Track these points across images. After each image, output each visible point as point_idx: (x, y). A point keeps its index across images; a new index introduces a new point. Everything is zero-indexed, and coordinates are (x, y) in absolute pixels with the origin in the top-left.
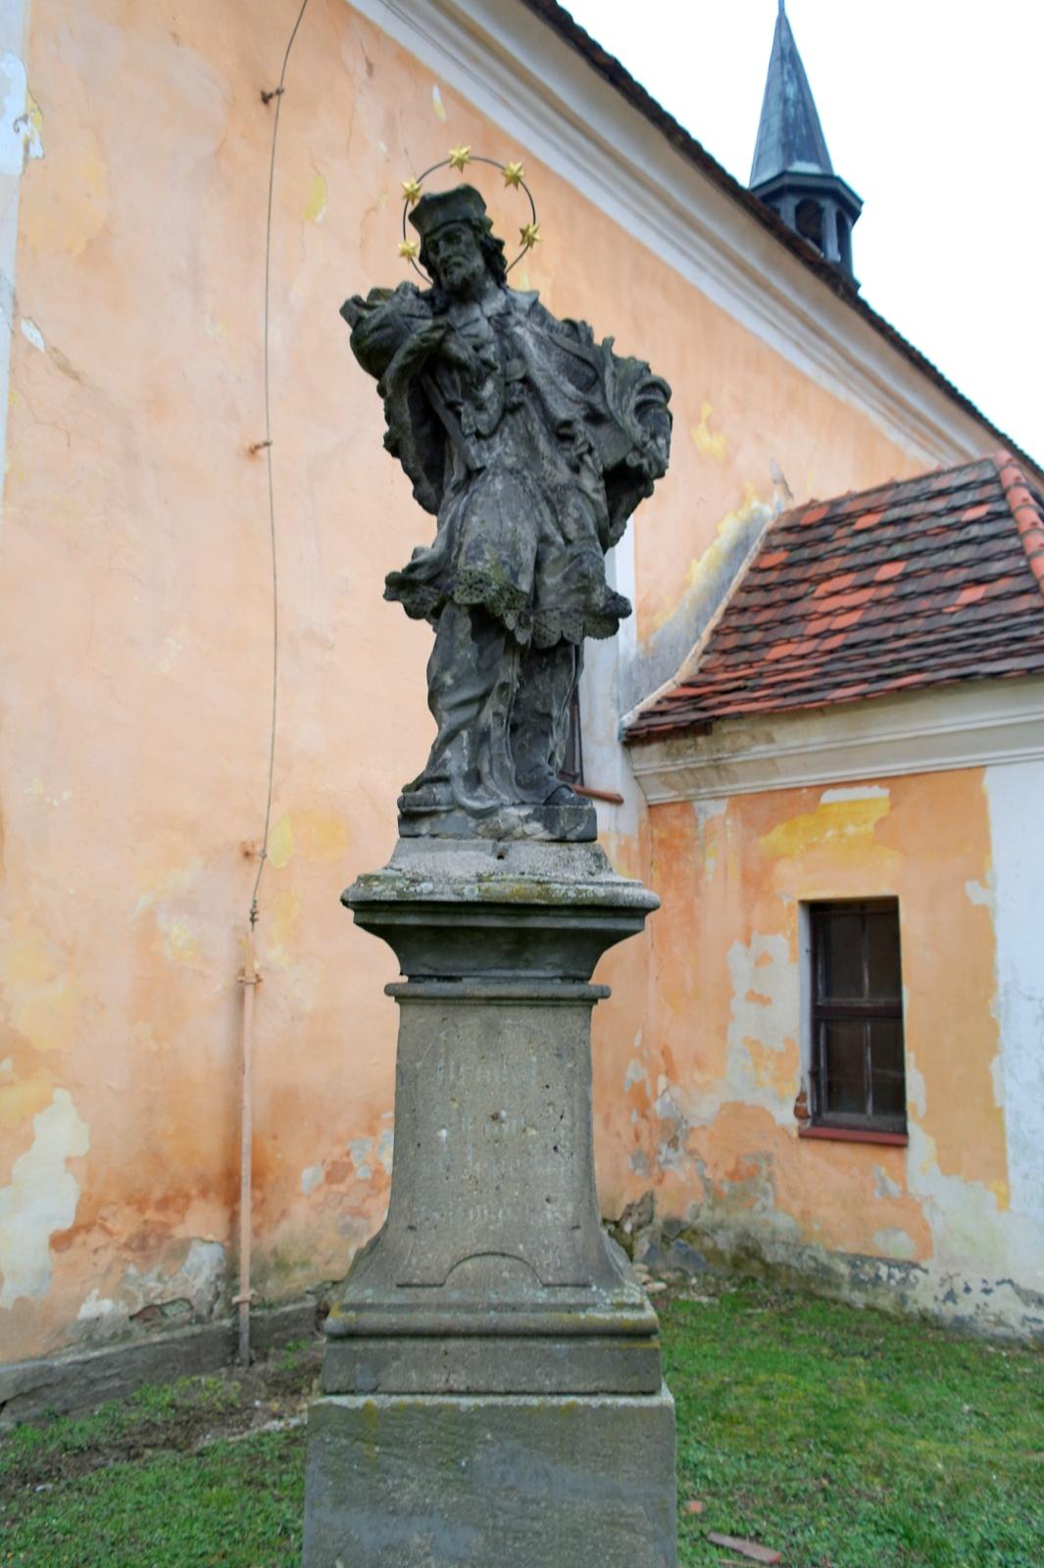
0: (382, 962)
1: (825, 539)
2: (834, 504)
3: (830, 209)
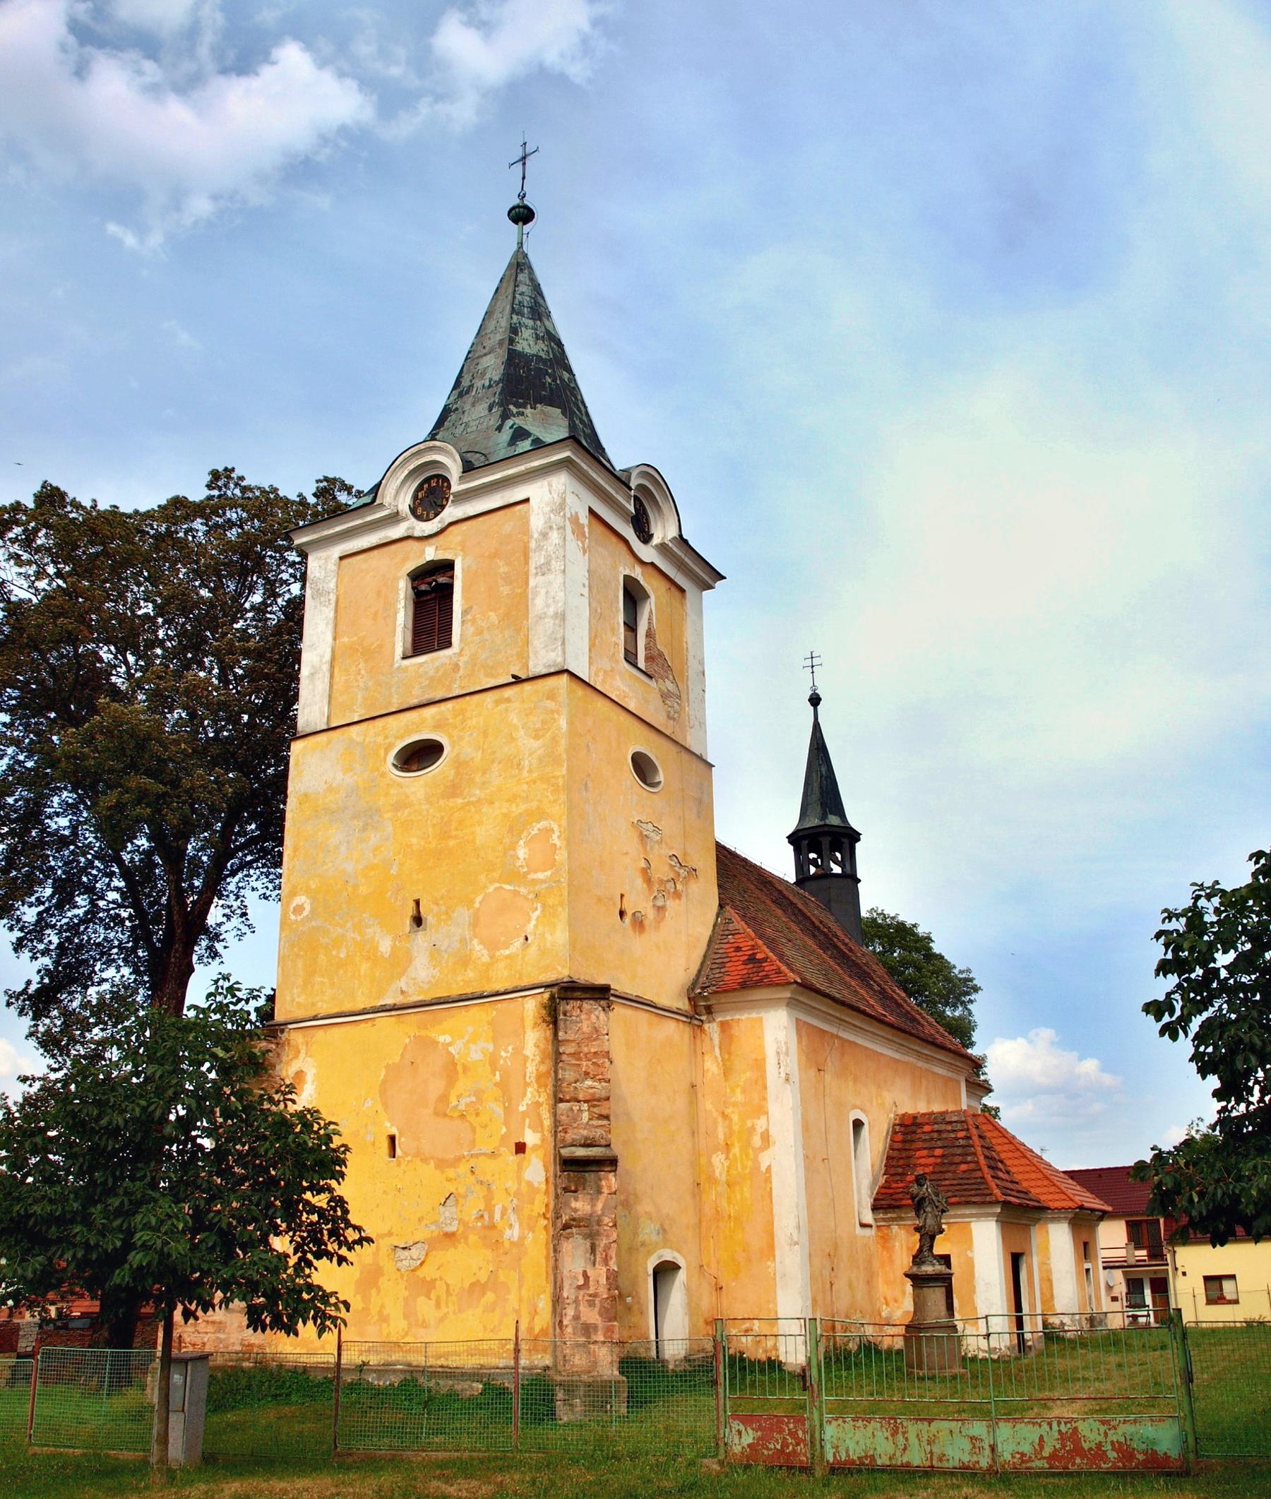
0: (909, 1283)
1: (914, 1132)
2: (915, 1118)
3: (846, 841)
